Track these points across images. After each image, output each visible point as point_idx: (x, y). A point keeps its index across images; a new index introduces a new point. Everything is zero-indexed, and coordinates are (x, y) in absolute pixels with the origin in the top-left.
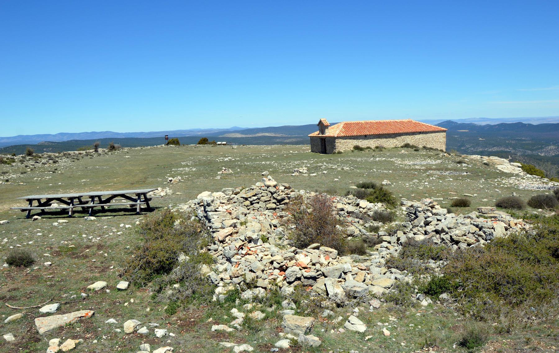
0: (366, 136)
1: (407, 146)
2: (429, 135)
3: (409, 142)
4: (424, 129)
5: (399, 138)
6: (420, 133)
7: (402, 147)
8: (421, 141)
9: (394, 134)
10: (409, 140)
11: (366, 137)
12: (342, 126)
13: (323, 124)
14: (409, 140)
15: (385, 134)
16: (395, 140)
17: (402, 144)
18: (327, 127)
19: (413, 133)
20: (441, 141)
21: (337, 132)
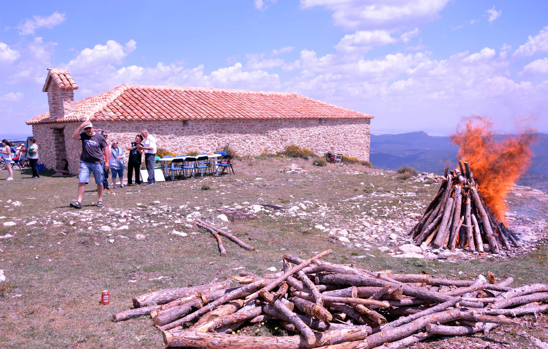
0: (185, 122)
1: (293, 153)
2: (338, 128)
3: (296, 144)
4: (329, 114)
5: (273, 133)
6: (321, 121)
7: (279, 154)
8: (322, 140)
9: (261, 120)
10: (297, 137)
11: (185, 125)
12: (118, 93)
13: (56, 85)
14: (297, 137)
15: (239, 119)
16: (262, 138)
17: (282, 148)
18: (68, 92)
19: (306, 122)
20: (362, 142)
21: (100, 106)
